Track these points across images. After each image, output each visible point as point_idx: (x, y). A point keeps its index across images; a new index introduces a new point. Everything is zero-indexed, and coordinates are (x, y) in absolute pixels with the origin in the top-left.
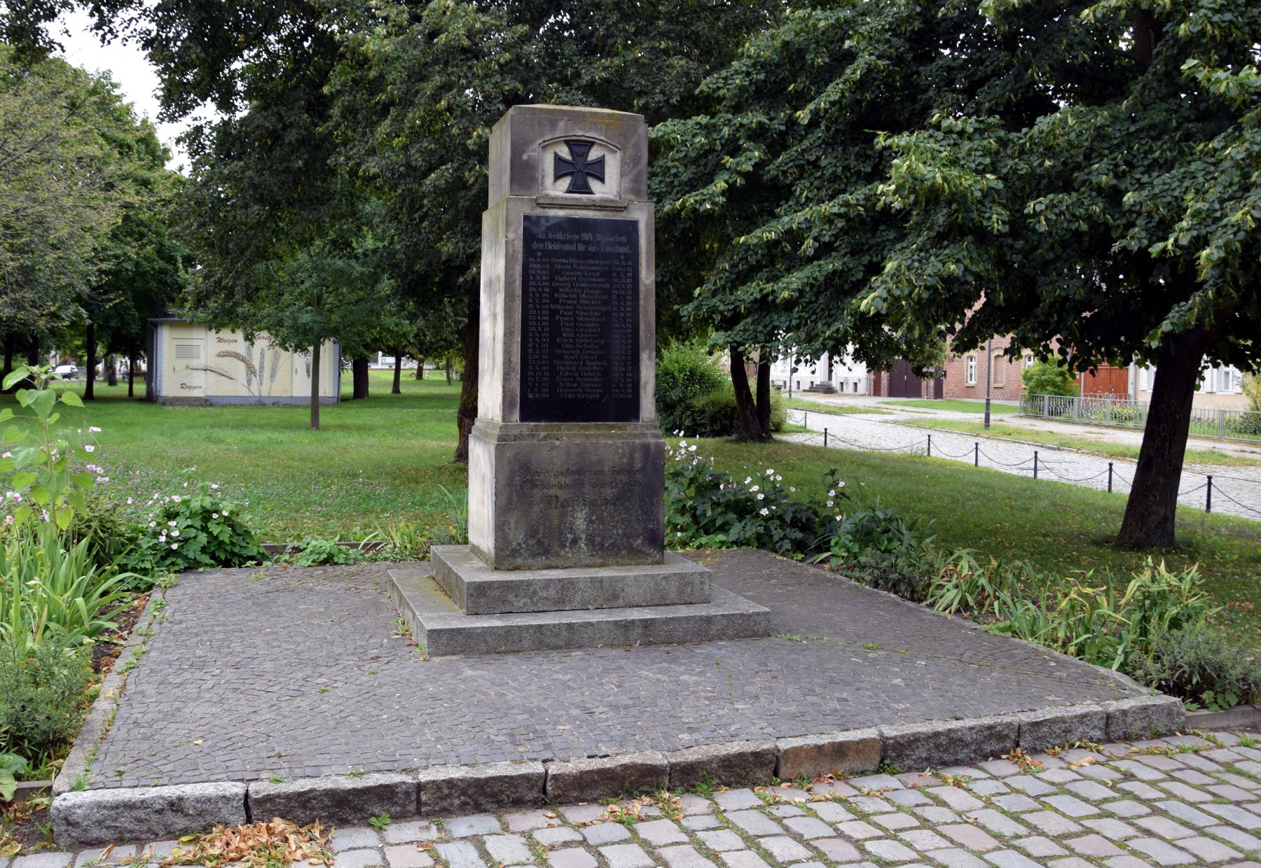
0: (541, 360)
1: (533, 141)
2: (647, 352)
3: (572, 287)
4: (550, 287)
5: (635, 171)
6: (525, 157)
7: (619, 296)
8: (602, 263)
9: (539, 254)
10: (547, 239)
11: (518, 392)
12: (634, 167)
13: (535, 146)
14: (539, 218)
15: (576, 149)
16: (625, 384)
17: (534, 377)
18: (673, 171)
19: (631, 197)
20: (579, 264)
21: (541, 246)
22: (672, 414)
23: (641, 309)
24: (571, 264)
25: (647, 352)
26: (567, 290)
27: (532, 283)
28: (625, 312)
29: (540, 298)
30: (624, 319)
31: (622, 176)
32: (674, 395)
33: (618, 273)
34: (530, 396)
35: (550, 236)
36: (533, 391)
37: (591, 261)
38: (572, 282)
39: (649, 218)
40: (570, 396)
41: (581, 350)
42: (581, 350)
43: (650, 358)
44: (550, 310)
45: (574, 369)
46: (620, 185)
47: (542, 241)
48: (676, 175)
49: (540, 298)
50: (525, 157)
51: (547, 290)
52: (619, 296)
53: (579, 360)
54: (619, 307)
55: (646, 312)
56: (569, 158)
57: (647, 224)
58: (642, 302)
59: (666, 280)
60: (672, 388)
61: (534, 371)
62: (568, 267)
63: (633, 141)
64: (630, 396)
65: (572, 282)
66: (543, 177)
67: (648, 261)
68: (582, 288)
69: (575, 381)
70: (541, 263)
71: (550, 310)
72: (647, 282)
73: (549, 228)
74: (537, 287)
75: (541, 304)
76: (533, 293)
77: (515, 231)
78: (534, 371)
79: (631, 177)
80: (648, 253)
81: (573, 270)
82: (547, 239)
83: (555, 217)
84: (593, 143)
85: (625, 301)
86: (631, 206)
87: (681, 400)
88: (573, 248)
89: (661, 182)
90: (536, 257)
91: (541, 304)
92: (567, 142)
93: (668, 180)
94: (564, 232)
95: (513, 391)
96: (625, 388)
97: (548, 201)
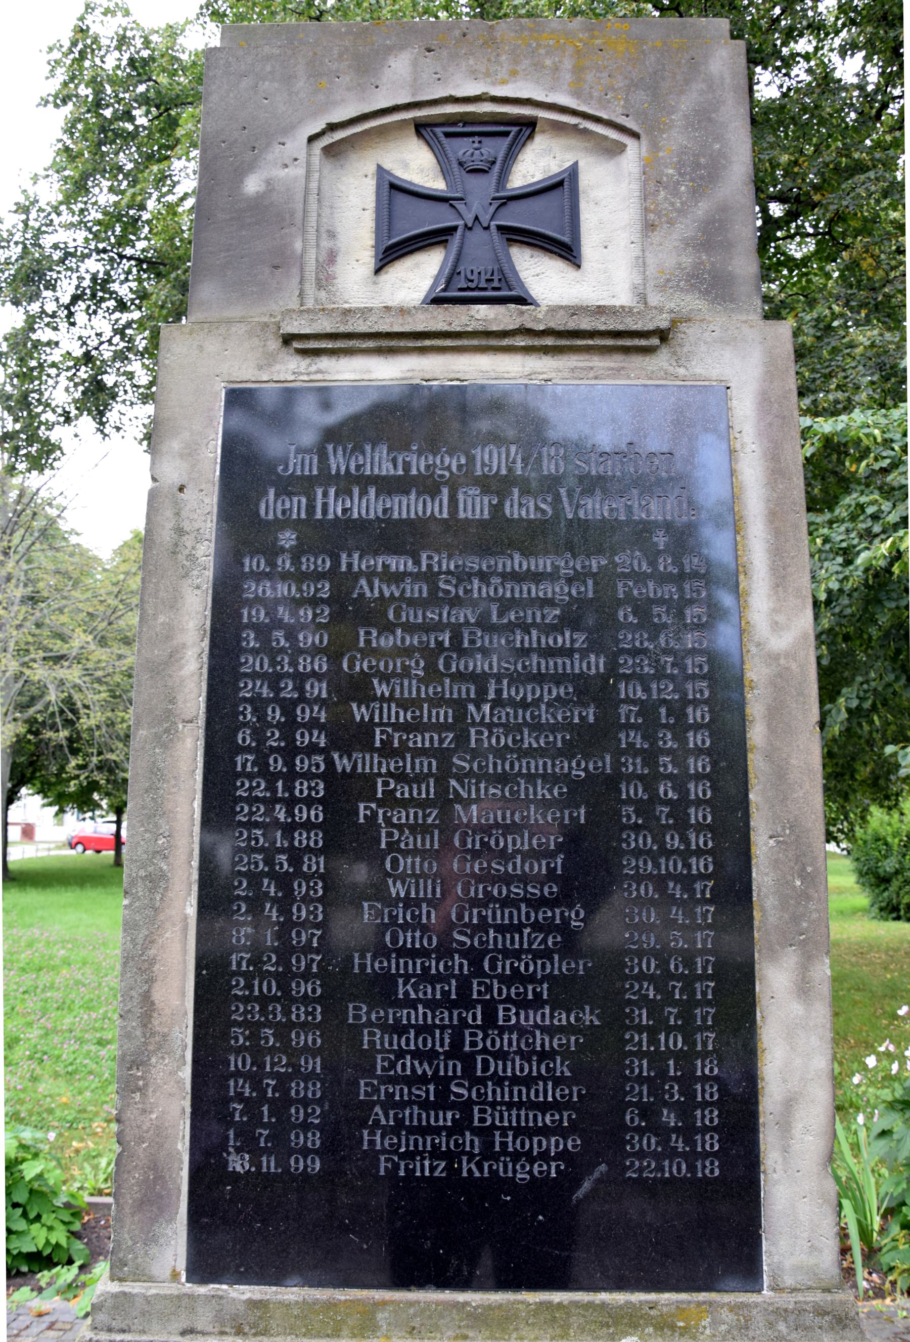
0: (287, 999)
1: (289, 129)
2: (790, 959)
3: (432, 674)
4: (334, 677)
5: (702, 208)
6: (253, 185)
7: (647, 709)
8: (565, 564)
9: (288, 539)
10: (325, 478)
11: (183, 1147)
12: (696, 193)
13: (297, 144)
14: (289, 395)
15: (462, 148)
16: (685, 1110)
17: (256, 1080)
18: (870, 510)
19: (691, 302)
20: (463, 576)
21: (297, 505)
22: (886, 889)
23: (756, 763)
24: (430, 577)
25: (790, 959)
26: (410, 689)
27: (251, 663)
28: (680, 784)
29: (289, 726)
30: (679, 808)
31: (648, 227)
32: (889, 865)
33: (642, 609)
34: (238, 1164)
35: (337, 462)
36: (248, 1144)
37: (517, 562)
38: (431, 654)
39: (771, 373)
40: (424, 1168)
41: (474, 956)
42: (474, 956)
43: (803, 989)
44: (330, 775)
45: (442, 1043)
46: (641, 263)
47: (306, 485)
48: (875, 517)
49: (289, 726)
50: (253, 185)
51: (318, 689)
52: (647, 709)
53: (464, 1001)
54: (651, 756)
55: (780, 774)
56: (438, 185)
57: (765, 401)
58: (757, 734)
59: (867, 705)
60: (886, 857)
61: (257, 1052)
62: (415, 590)
63: (686, 103)
64: (712, 1169)
65: (431, 654)
66: (332, 257)
67: (777, 553)
68: (480, 680)
69: (443, 1102)
70: (300, 577)
71: (330, 775)
72: (780, 643)
73: (332, 435)
74: (274, 681)
75: (290, 752)
76: (259, 704)
77: (190, 453)
78: (257, 1052)
79: (685, 228)
80: (774, 516)
81: (434, 599)
82: (325, 478)
83: (357, 389)
84: (529, 126)
85: (680, 728)
86: (690, 333)
87: (897, 872)
88: (439, 508)
89: (848, 531)
90: (272, 552)
91: (290, 752)
92: (421, 128)
93: (862, 526)
94: (399, 445)
95: (160, 1133)
96: (688, 1131)
97: (326, 325)
